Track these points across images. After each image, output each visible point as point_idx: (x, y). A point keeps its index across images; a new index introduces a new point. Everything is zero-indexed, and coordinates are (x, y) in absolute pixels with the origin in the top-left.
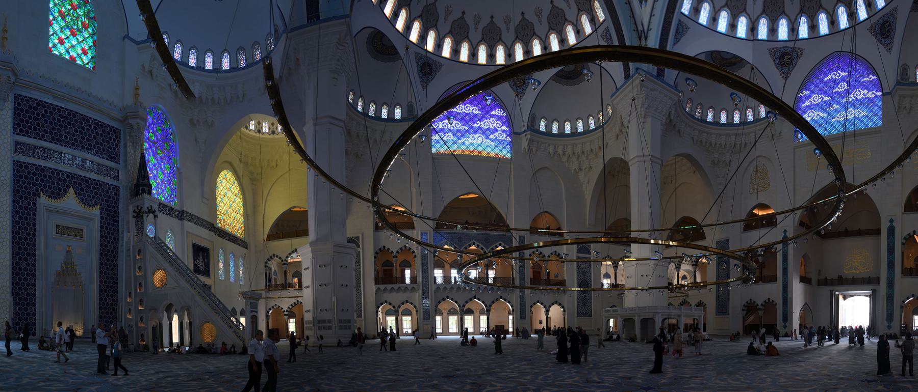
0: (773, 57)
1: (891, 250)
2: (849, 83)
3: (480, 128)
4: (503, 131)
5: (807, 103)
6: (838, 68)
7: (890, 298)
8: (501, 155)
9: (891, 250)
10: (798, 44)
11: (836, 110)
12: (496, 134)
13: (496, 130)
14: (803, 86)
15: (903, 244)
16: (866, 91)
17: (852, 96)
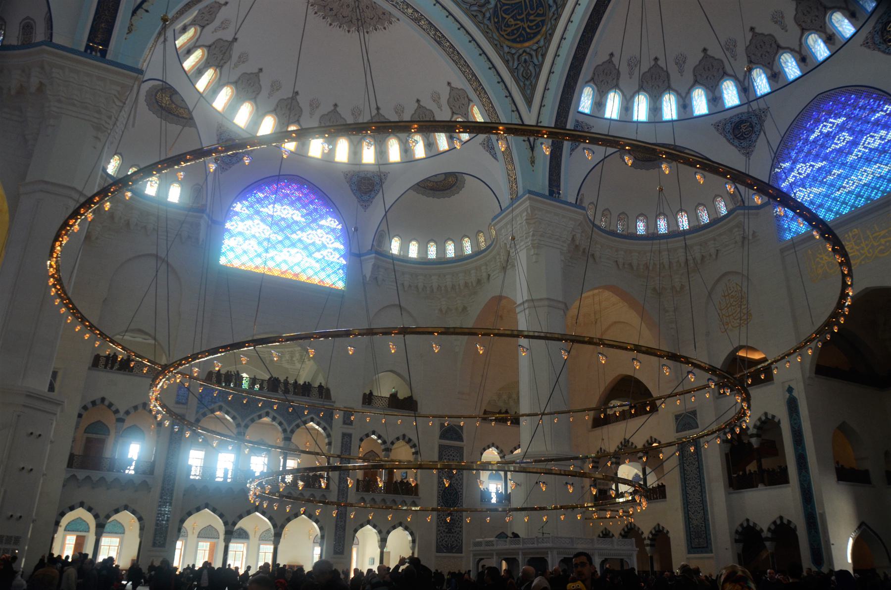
2: (851, 131)
3: (300, 240)
4: (336, 249)
6: (829, 114)
8: (328, 282)
11: (839, 175)
12: (324, 252)
13: (324, 246)
14: (778, 157)
16: (883, 133)
17: (860, 148)
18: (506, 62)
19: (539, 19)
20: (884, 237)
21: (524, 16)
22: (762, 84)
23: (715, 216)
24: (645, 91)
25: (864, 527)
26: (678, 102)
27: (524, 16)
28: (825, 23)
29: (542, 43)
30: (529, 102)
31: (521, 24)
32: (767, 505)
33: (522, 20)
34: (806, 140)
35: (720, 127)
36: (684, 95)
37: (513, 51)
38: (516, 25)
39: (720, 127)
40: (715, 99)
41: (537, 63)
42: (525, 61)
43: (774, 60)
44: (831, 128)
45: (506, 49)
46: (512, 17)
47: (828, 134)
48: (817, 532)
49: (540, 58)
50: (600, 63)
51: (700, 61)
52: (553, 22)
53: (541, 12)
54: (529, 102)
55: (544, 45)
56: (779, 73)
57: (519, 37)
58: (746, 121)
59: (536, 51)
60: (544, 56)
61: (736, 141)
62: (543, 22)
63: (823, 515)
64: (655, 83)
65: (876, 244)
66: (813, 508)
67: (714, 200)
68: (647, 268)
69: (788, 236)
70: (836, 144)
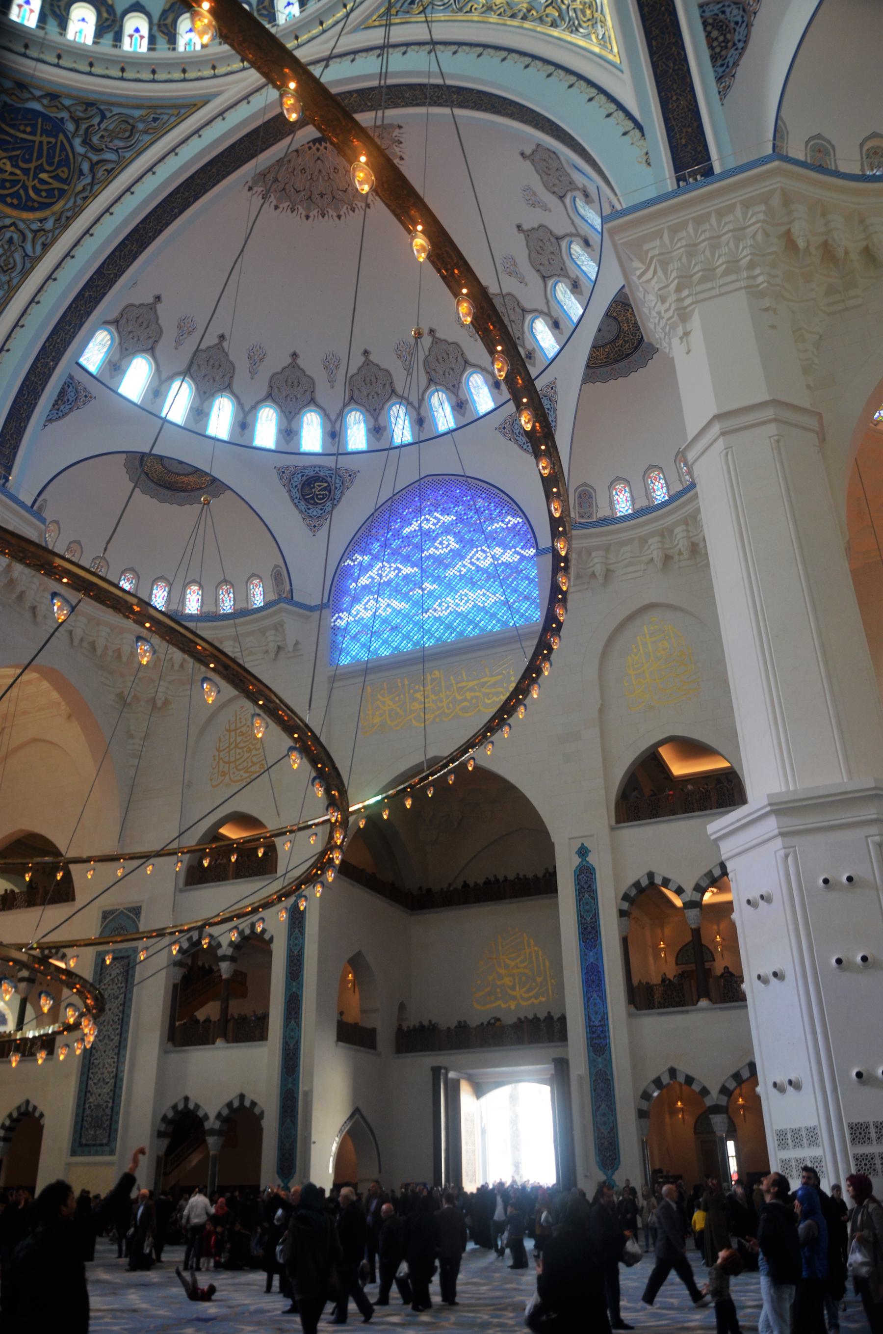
0: (288, 484)
1: (589, 932)
2: (460, 540)
5: (364, 581)
6: (436, 506)
7: (602, 1084)
9: (589, 932)
10: (343, 462)
11: (431, 593)
15: (622, 913)
16: (498, 550)
17: (466, 562)
19: (56, 184)
20: (472, 690)
21: (32, 166)
22: (357, 435)
23: (244, 605)
24: (192, 378)
25: (357, 1116)
26: (236, 416)
27: (32, 166)
28: (460, 382)
29: (49, 225)
31: (22, 177)
32: (225, 1073)
33: (26, 172)
34: (397, 534)
35: (286, 475)
36: (247, 408)
38: (12, 174)
39: (286, 475)
40: (289, 432)
42: (11, 241)
43: (382, 408)
44: (434, 524)
46: (10, 158)
47: (428, 533)
48: (294, 1123)
49: (38, 248)
50: (137, 303)
51: (284, 369)
52: (79, 202)
53: (65, 176)
55: (52, 231)
56: (385, 428)
57: (11, 195)
58: (323, 480)
59: (35, 232)
60: (46, 247)
61: (303, 502)
62: (62, 192)
63: (308, 1095)
64: (211, 370)
65: (459, 697)
66: (296, 1082)
67: (248, 580)
68: (119, 657)
69: (345, 661)
70: (436, 548)
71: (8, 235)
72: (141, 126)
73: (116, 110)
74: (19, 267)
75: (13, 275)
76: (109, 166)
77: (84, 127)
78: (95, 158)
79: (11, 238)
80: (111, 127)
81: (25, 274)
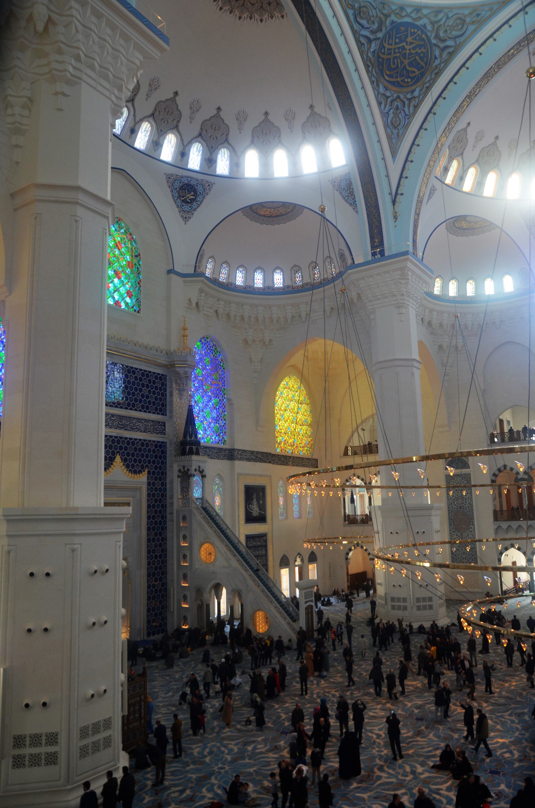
18: (379, 104)
29: (416, 93)
30: (394, 153)
37: (388, 94)
41: (407, 113)
45: (382, 90)
54: (394, 153)
55: (419, 97)
59: (410, 100)
60: (416, 107)
71: (396, 104)
72: (468, 20)
73: (455, 12)
74: (402, 123)
75: (400, 128)
76: (451, 50)
77: (436, 27)
78: (442, 45)
79: (397, 106)
80: (451, 24)
81: (407, 127)
